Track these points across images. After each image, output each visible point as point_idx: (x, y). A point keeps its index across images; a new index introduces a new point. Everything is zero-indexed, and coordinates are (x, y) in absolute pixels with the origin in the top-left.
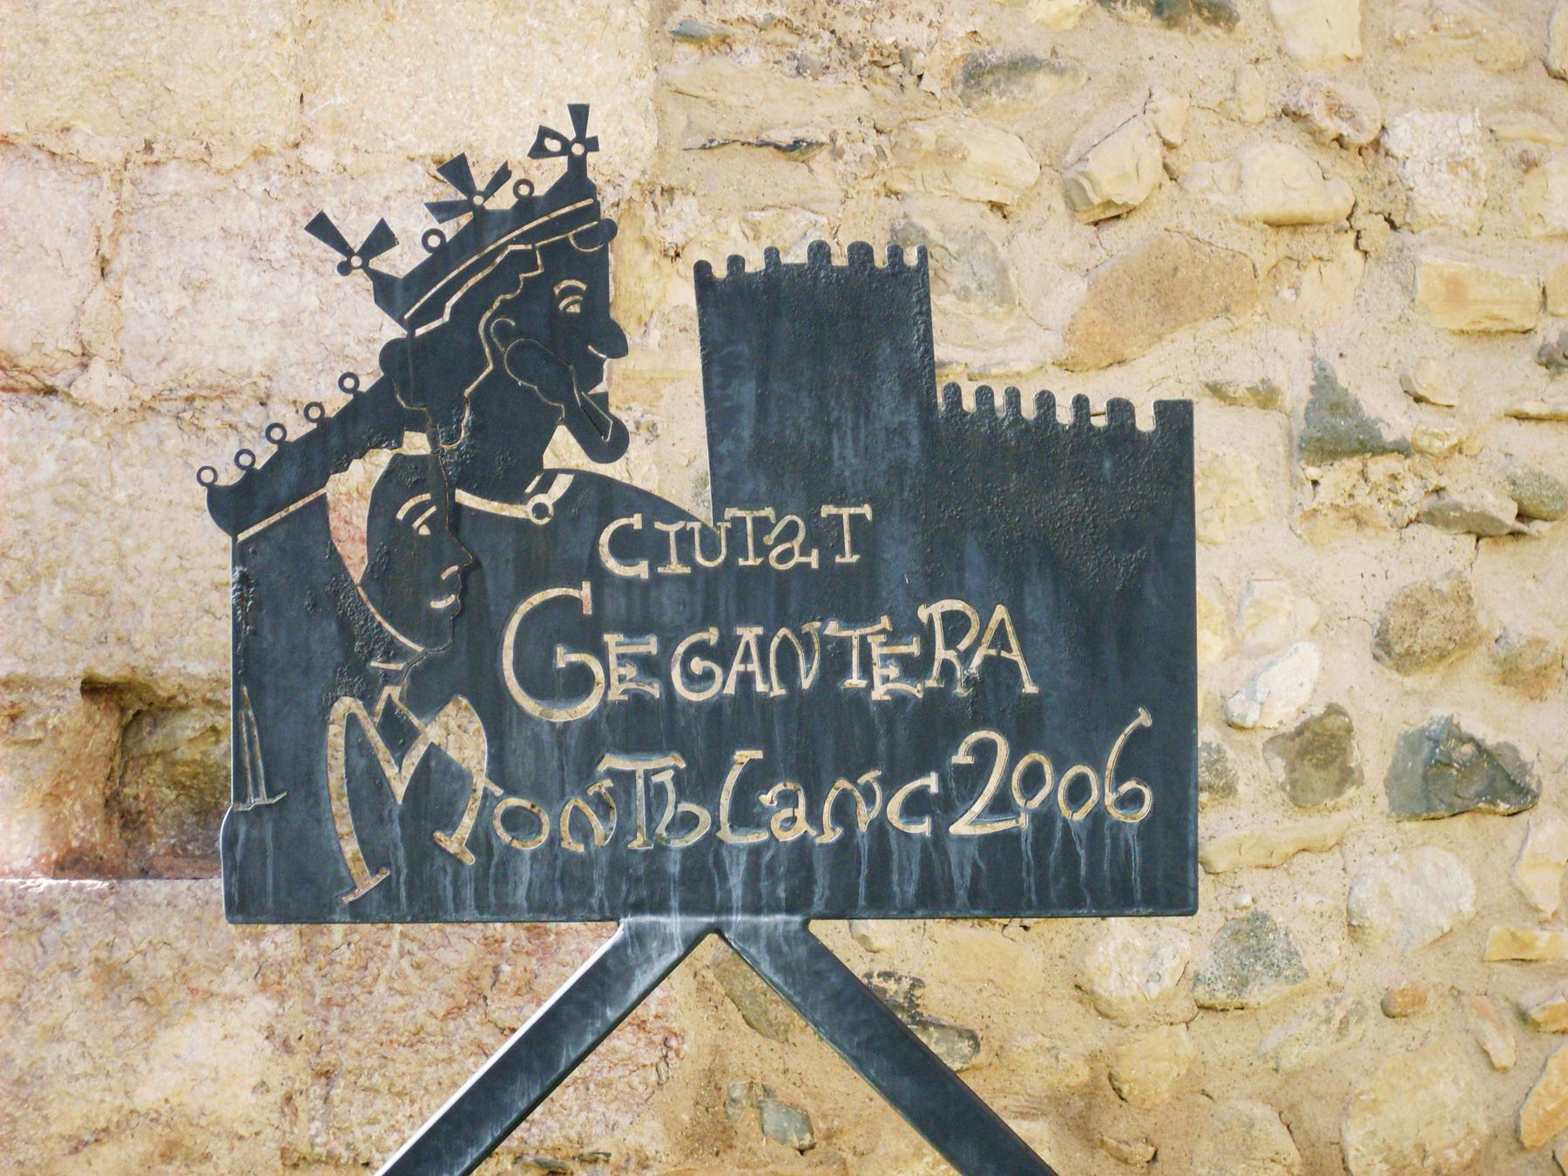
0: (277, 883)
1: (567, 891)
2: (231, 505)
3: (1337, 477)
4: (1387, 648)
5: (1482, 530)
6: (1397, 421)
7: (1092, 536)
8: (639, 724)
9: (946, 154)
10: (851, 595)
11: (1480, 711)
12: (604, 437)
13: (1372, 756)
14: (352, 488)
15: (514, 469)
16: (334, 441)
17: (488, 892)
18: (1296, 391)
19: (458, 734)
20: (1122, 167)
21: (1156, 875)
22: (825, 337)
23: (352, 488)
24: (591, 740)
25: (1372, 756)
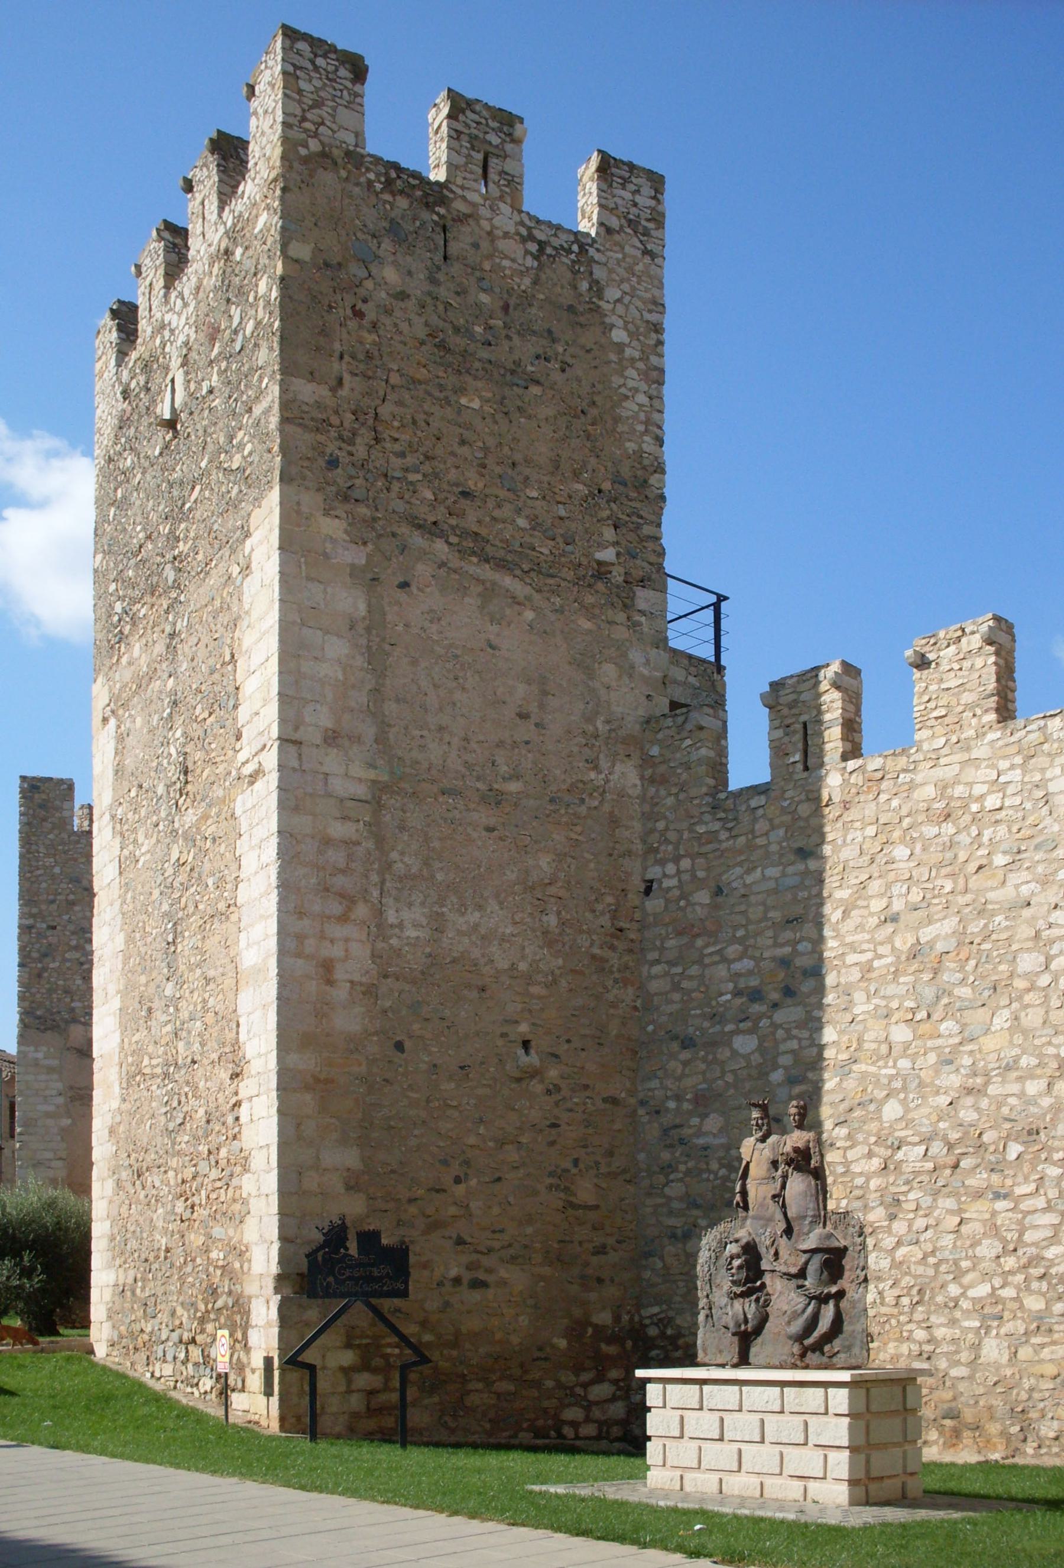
0: (312, 1294)
1: (343, 1296)
2: (307, 1256)
3: (460, 1248)
4: (469, 1268)
5: (481, 1253)
6: (469, 1240)
7: (397, 1260)
8: (350, 1278)
9: (406, 1211)
10: (372, 1265)
11: (482, 1276)
12: (347, 1249)
13: (465, 1282)
14: (320, 1253)
15: (337, 1252)
16: (318, 1250)
17: (335, 1295)
18: (455, 1236)
19: (331, 1279)
20: (430, 1211)
21: (404, 1294)
22: (369, 1239)
23: (320, 1253)
24: (344, 1281)
25: (465, 1282)
